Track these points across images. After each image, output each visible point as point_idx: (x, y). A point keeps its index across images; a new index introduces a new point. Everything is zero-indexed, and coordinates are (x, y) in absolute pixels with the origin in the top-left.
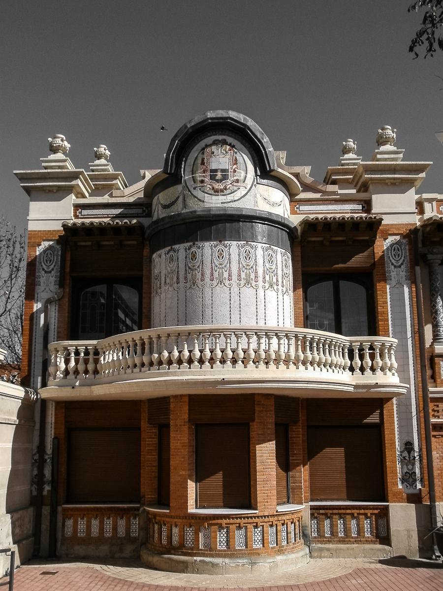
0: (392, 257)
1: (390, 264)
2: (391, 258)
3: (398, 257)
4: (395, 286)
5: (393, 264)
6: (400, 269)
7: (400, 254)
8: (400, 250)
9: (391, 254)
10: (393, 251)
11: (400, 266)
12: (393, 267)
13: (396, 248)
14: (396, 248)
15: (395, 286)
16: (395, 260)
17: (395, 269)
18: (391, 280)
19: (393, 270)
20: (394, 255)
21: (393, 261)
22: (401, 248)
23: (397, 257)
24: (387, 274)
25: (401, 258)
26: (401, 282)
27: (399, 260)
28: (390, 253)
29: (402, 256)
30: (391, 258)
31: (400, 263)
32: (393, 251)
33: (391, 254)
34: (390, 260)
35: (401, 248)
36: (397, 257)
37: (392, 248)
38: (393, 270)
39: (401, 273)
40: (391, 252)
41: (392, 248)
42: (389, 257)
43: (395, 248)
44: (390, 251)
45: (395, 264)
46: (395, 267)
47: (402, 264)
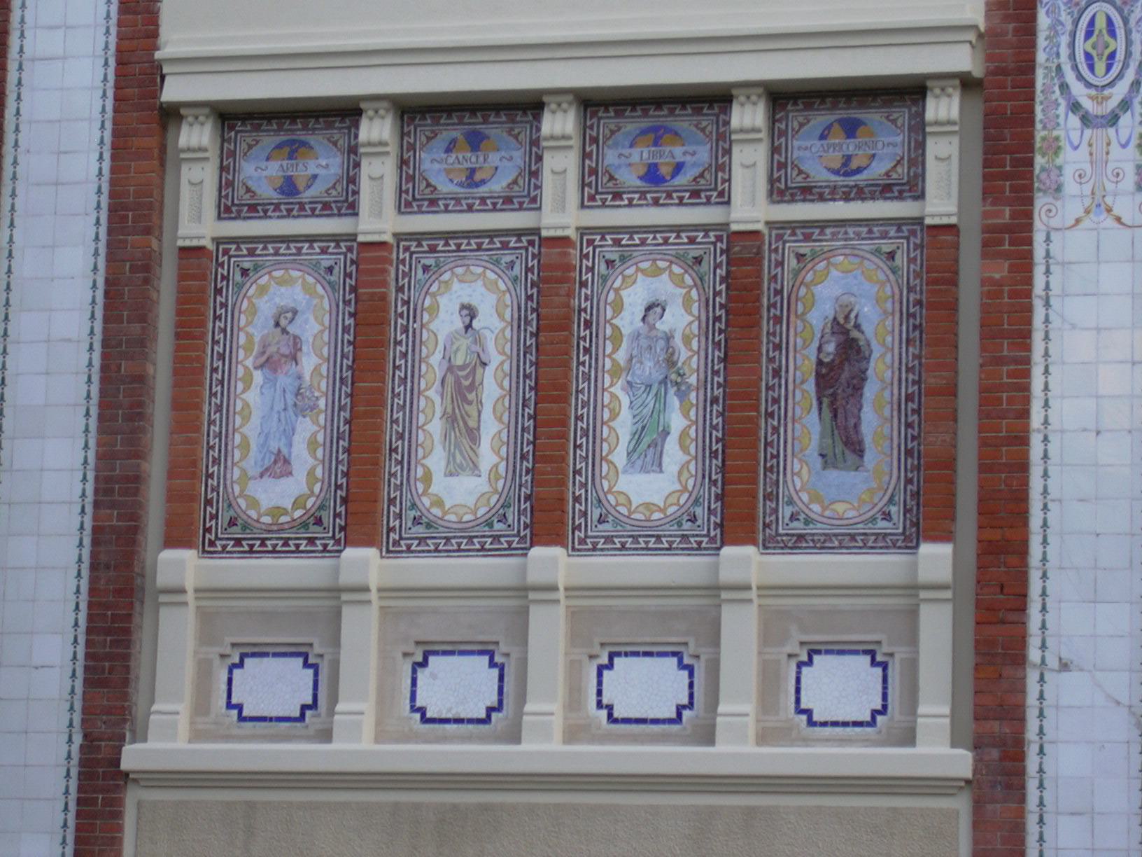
0: (1075, 68)
1: (1062, 110)
2: (1070, 77)
3: (1109, 68)
4: (1078, 221)
5: (1075, 107)
6: (1111, 131)
7: (1120, 56)
8: (1120, 33)
9: (1072, 56)
10: (1080, 35)
11: (1113, 119)
12: (1074, 121)
13: (1101, 23)
14: (1101, 23)
15: (1078, 221)
16: (1089, 85)
17: (1088, 132)
18: (1059, 189)
19: (1075, 136)
20: (1088, 56)
21: (1077, 89)
22: (1126, 21)
23: (1100, 66)
24: (1039, 161)
25: (1120, 76)
26: (1109, 200)
27: (1111, 84)
28: (1064, 52)
29: (1125, 66)
30: (1070, 77)
31: (1113, 103)
32: (1080, 35)
33: (1072, 56)
34: (1064, 87)
35: (1126, 21)
36: (1100, 66)
37: (1076, 23)
38: (1075, 136)
39: (1115, 149)
40: (1072, 45)
41: (1076, 23)
42: (1059, 67)
43: (1092, 23)
44: (1064, 40)
45: (1087, 104)
46: (1086, 120)
47: (1125, 105)
